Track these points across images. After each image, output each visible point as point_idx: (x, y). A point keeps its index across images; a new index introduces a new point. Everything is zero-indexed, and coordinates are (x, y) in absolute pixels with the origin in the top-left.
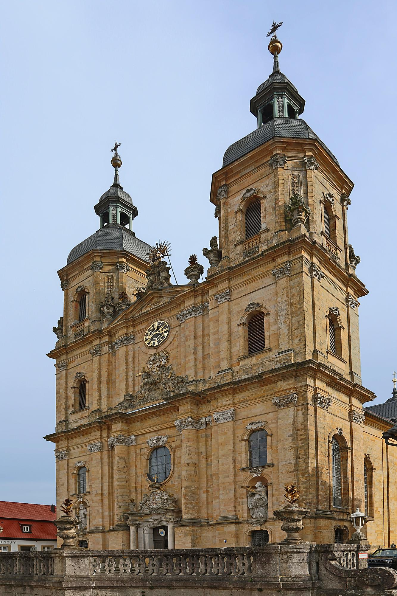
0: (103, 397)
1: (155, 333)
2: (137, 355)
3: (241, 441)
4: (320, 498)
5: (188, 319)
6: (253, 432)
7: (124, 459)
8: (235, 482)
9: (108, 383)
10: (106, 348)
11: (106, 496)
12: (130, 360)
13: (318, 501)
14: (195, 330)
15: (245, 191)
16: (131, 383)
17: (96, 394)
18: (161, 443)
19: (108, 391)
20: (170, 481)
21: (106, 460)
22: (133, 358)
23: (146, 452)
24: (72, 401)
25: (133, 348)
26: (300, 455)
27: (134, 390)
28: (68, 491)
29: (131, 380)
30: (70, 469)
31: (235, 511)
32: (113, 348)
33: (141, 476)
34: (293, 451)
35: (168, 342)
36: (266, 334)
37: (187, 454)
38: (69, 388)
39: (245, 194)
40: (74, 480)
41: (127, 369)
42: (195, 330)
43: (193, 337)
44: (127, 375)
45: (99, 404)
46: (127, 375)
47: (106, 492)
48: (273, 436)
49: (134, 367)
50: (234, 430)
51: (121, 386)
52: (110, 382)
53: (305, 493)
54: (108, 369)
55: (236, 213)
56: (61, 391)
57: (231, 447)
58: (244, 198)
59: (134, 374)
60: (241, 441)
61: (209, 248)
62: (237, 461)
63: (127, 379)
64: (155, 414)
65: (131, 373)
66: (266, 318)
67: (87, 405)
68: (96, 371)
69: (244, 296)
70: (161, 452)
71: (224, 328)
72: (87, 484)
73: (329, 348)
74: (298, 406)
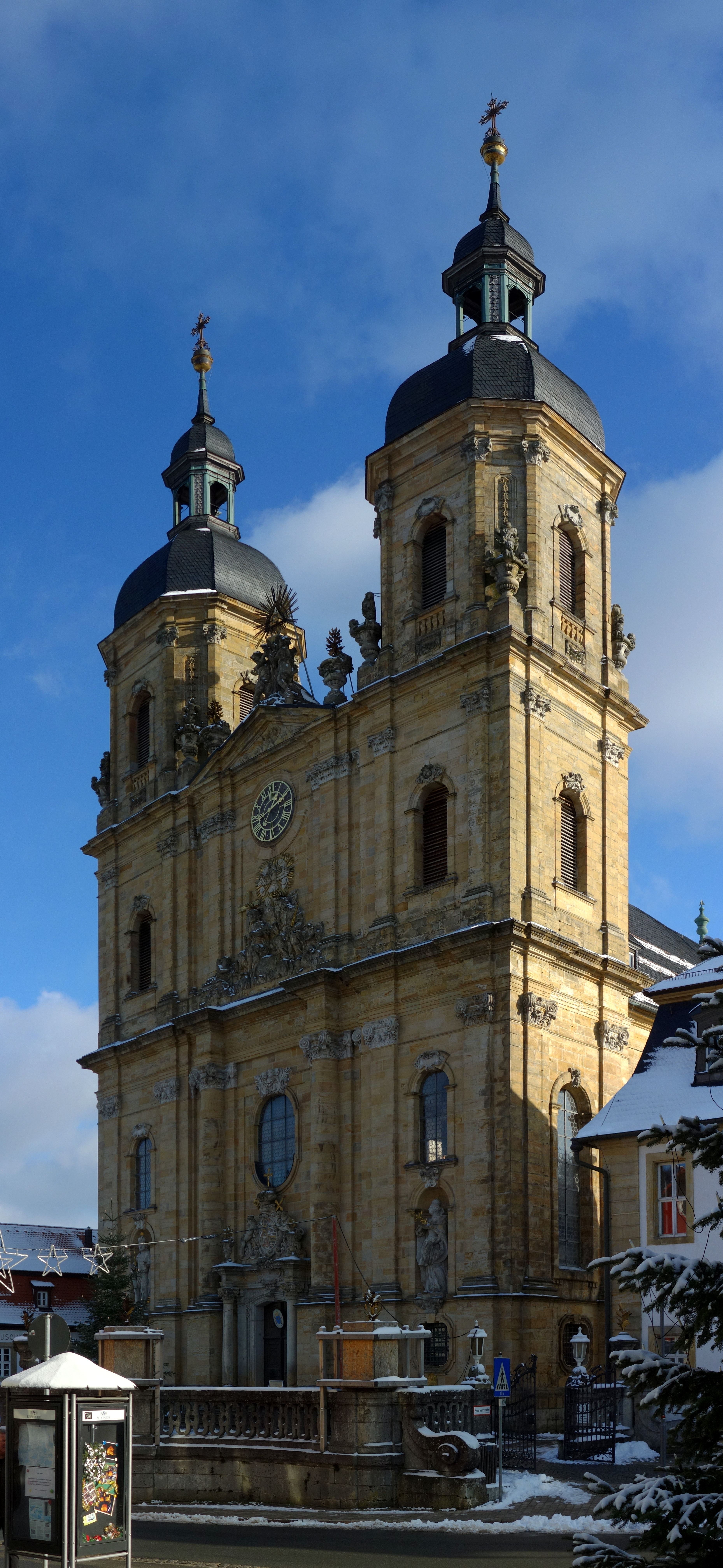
0: (180, 963)
1: (269, 810)
2: (239, 859)
3: (406, 1095)
4: (531, 1249)
5: (324, 784)
6: (427, 1074)
7: (217, 1126)
8: (397, 1198)
9: (189, 928)
10: (185, 837)
11: (184, 1218)
12: (228, 871)
13: (527, 1256)
14: (337, 810)
15: (420, 502)
16: (228, 930)
17: (168, 954)
18: (278, 1087)
19: (190, 945)
20: (293, 1186)
21: (184, 1124)
22: (233, 867)
23: (253, 1106)
24: (126, 969)
25: (233, 842)
26: (497, 1143)
27: (233, 948)
28: (119, 1203)
29: (228, 921)
30: (124, 1142)
31: (397, 1271)
32: (197, 837)
33: (245, 1167)
34: (486, 1129)
35: (291, 835)
36: (450, 841)
37: (320, 1120)
38: (121, 934)
39: (420, 507)
40: (129, 1172)
41: (222, 893)
42: (337, 810)
43: (331, 829)
44: (222, 909)
45: (175, 983)
46: (222, 909)
47: (184, 1207)
48: (456, 1089)
49: (233, 890)
50: (396, 1068)
51: (211, 934)
52: (193, 923)
53: (505, 1235)
54: (189, 890)
55: (405, 546)
56: (108, 941)
57: (390, 1110)
58: (418, 515)
59: (233, 907)
60: (406, 1095)
61: (361, 620)
62: (400, 1144)
63: (222, 919)
64: (268, 1014)
65: (228, 904)
66: (450, 803)
67: (152, 980)
68: (169, 895)
69: (417, 743)
70: (278, 1108)
71: (383, 816)
72: (153, 1186)
73: (559, 875)
74: (497, 1022)
